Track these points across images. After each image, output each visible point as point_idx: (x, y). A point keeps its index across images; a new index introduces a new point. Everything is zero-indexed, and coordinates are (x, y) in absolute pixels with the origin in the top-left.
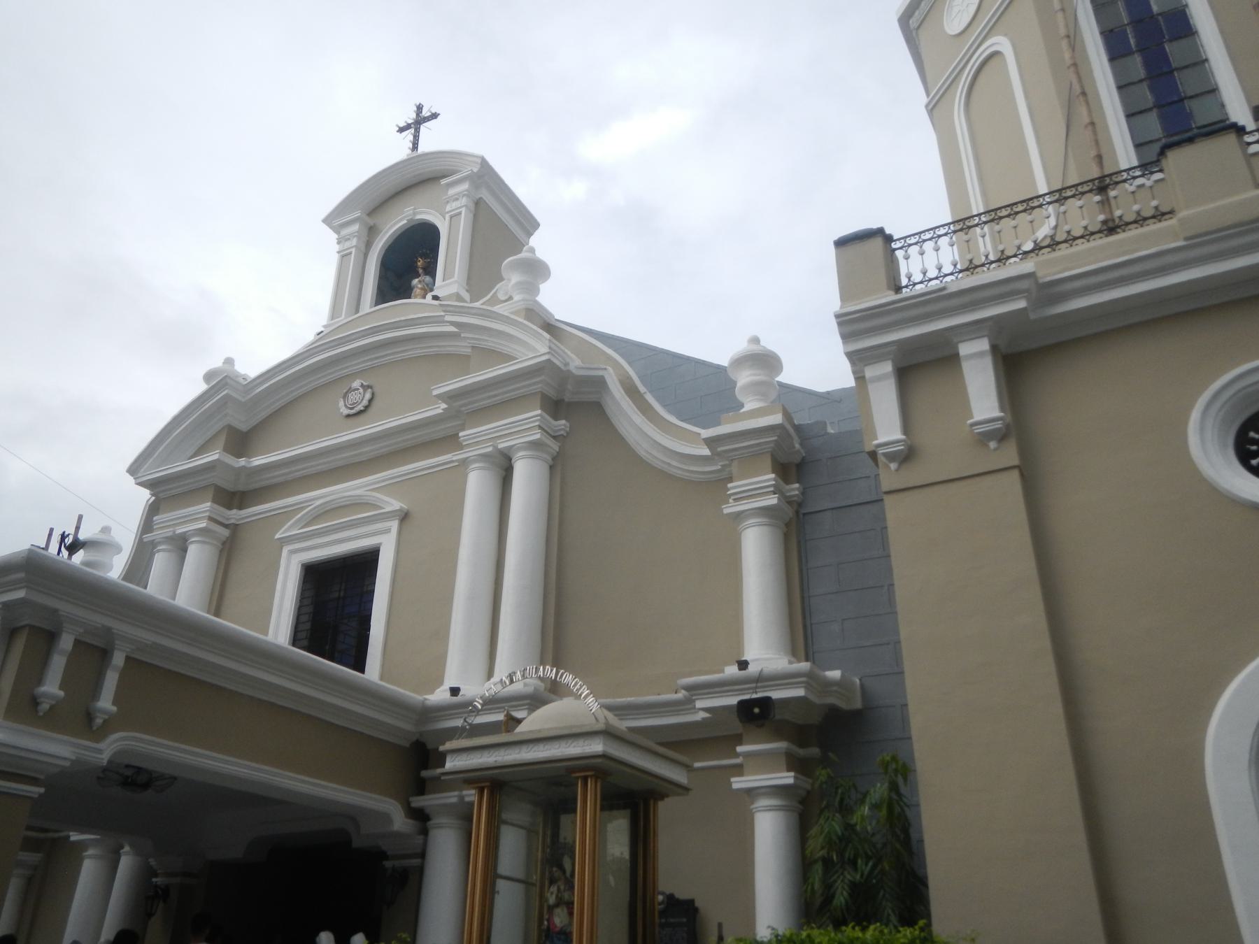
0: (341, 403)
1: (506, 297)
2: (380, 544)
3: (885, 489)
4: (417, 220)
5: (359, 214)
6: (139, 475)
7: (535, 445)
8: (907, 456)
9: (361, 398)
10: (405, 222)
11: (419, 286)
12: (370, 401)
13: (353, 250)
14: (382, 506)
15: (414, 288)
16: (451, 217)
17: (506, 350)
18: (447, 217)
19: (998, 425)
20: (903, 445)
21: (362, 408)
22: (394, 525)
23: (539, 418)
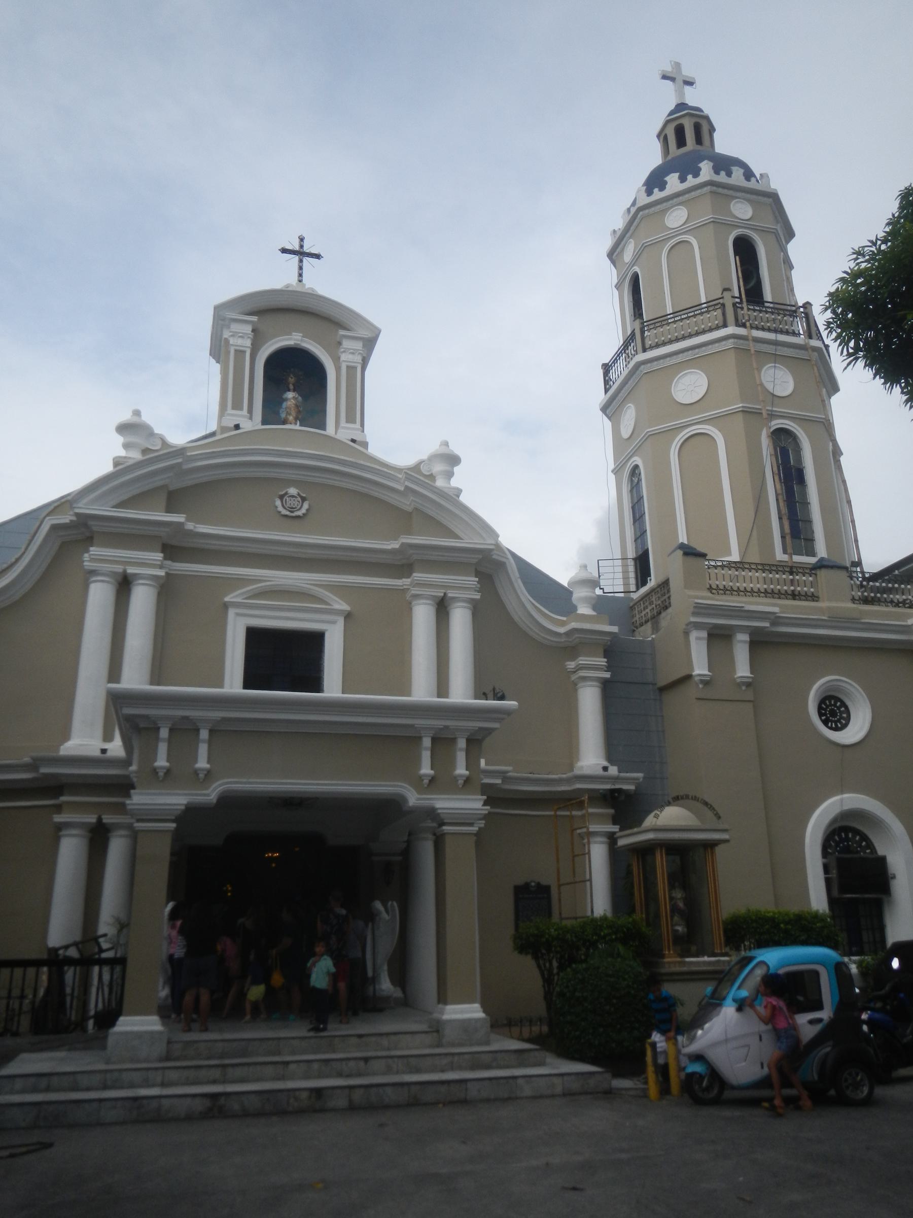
0: (278, 503)
1: (428, 474)
2: (327, 630)
5: (256, 320)
6: (80, 505)
7: (472, 601)
8: (706, 683)
9: (298, 508)
11: (292, 400)
12: (307, 510)
14: (331, 603)
15: (286, 400)
17: (445, 522)
19: (750, 680)
21: (301, 515)
22: (341, 621)
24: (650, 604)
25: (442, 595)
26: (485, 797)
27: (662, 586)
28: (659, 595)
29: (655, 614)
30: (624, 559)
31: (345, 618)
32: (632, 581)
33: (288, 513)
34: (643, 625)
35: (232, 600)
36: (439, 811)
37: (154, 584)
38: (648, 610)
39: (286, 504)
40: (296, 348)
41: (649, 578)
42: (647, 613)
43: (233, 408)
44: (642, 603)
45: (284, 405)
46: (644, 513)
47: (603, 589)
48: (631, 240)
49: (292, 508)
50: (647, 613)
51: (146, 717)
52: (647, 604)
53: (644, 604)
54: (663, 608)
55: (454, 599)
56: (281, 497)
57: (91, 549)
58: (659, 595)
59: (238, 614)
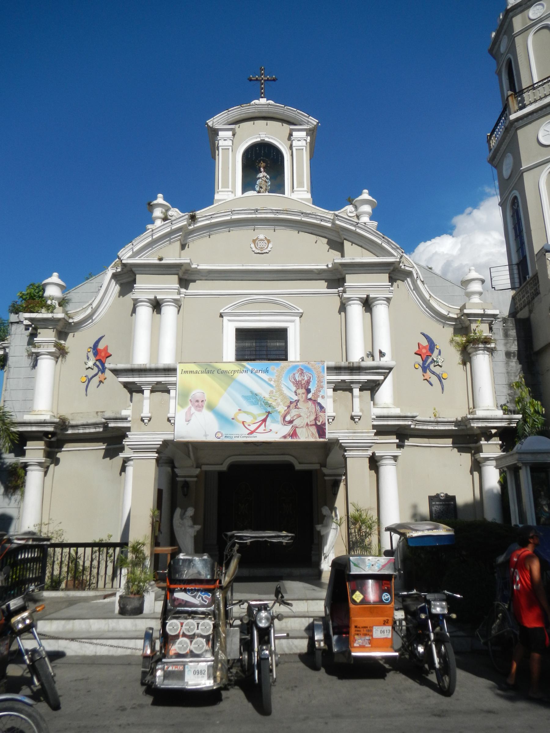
0: (253, 245)
9: (266, 247)
10: (259, 140)
21: (268, 252)
24: (526, 293)
25: (365, 296)
26: (375, 431)
27: (533, 279)
28: (532, 285)
29: (530, 299)
30: (510, 265)
31: (300, 317)
32: (517, 280)
33: (260, 251)
34: (522, 309)
36: (341, 441)
37: (175, 305)
38: (525, 298)
39: (257, 245)
40: (262, 143)
41: (527, 276)
42: (525, 300)
43: (222, 188)
44: (520, 293)
45: (258, 182)
46: (522, 230)
47: (494, 288)
48: (505, 37)
49: (261, 248)
50: (525, 300)
51: (133, 383)
52: (524, 293)
53: (522, 294)
54: (536, 294)
55: (375, 299)
56: (254, 241)
57: (135, 285)
58: (532, 285)
59: (229, 321)
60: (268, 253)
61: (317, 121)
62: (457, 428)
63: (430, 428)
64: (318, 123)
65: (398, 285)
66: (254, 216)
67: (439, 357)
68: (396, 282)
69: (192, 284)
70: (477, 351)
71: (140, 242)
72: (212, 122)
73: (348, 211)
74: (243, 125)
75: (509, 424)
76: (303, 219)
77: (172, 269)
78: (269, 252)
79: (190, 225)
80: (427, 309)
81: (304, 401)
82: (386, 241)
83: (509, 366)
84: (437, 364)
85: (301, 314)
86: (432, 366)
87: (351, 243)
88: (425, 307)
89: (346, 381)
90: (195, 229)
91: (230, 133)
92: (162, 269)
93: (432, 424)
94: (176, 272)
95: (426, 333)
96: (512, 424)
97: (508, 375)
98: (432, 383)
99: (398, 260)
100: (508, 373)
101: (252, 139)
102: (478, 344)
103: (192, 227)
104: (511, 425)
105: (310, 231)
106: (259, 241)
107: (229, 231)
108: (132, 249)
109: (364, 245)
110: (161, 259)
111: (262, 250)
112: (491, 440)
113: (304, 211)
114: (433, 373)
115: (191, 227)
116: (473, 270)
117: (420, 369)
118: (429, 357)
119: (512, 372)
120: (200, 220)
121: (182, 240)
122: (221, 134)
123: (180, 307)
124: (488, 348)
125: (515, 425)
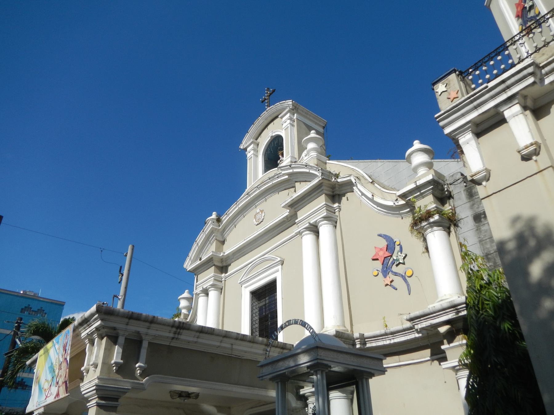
0: (254, 220)
3: (481, 197)
4: (274, 136)
7: (326, 218)
9: (261, 218)
10: (270, 138)
13: (252, 156)
16: (285, 130)
18: (284, 130)
20: (485, 172)
23: (325, 205)
25: (308, 224)
31: (282, 265)
35: (240, 281)
40: (273, 138)
59: (246, 287)
60: (263, 221)
61: (291, 100)
62: (420, 335)
63: (388, 342)
64: (292, 101)
65: (347, 198)
66: (249, 198)
67: (399, 254)
68: (345, 196)
69: (230, 268)
70: (425, 231)
71: (192, 254)
72: (242, 145)
73: (304, 157)
74: (262, 135)
75: (458, 313)
76: (273, 182)
77: (209, 264)
78: (264, 220)
79: (219, 226)
80: (378, 208)
81: (63, 362)
82: (310, 167)
83: (481, 232)
84: (398, 262)
85: (280, 262)
86: (394, 269)
87: (299, 183)
88: (376, 206)
89: (89, 333)
90: (224, 227)
91: (252, 146)
92: (206, 266)
93: (388, 338)
94: (212, 264)
95: (383, 233)
96: (460, 312)
97: (482, 244)
98: (396, 287)
99: (320, 178)
100: (480, 241)
101: (267, 139)
102: (420, 222)
103: (221, 226)
104: (461, 314)
105: (283, 188)
106: (257, 214)
107: (244, 217)
108: (190, 259)
109: (307, 180)
110: (200, 259)
111: (258, 221)
112: (455, 340)
113: (271, 176)
114: (396, 274)
115: (220, 227)
116: (416, 143)
117: (381, 274)
118: (389, 258)
119: (487, 238)
120: (223, 219)
121: (218, 238)
122: (248, 149)
123: (222, 289)
124: (434, 222)
125: (465, 313)
